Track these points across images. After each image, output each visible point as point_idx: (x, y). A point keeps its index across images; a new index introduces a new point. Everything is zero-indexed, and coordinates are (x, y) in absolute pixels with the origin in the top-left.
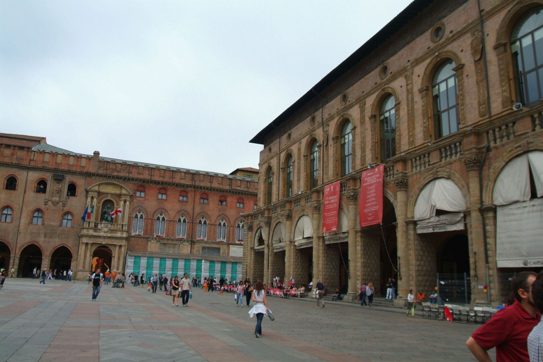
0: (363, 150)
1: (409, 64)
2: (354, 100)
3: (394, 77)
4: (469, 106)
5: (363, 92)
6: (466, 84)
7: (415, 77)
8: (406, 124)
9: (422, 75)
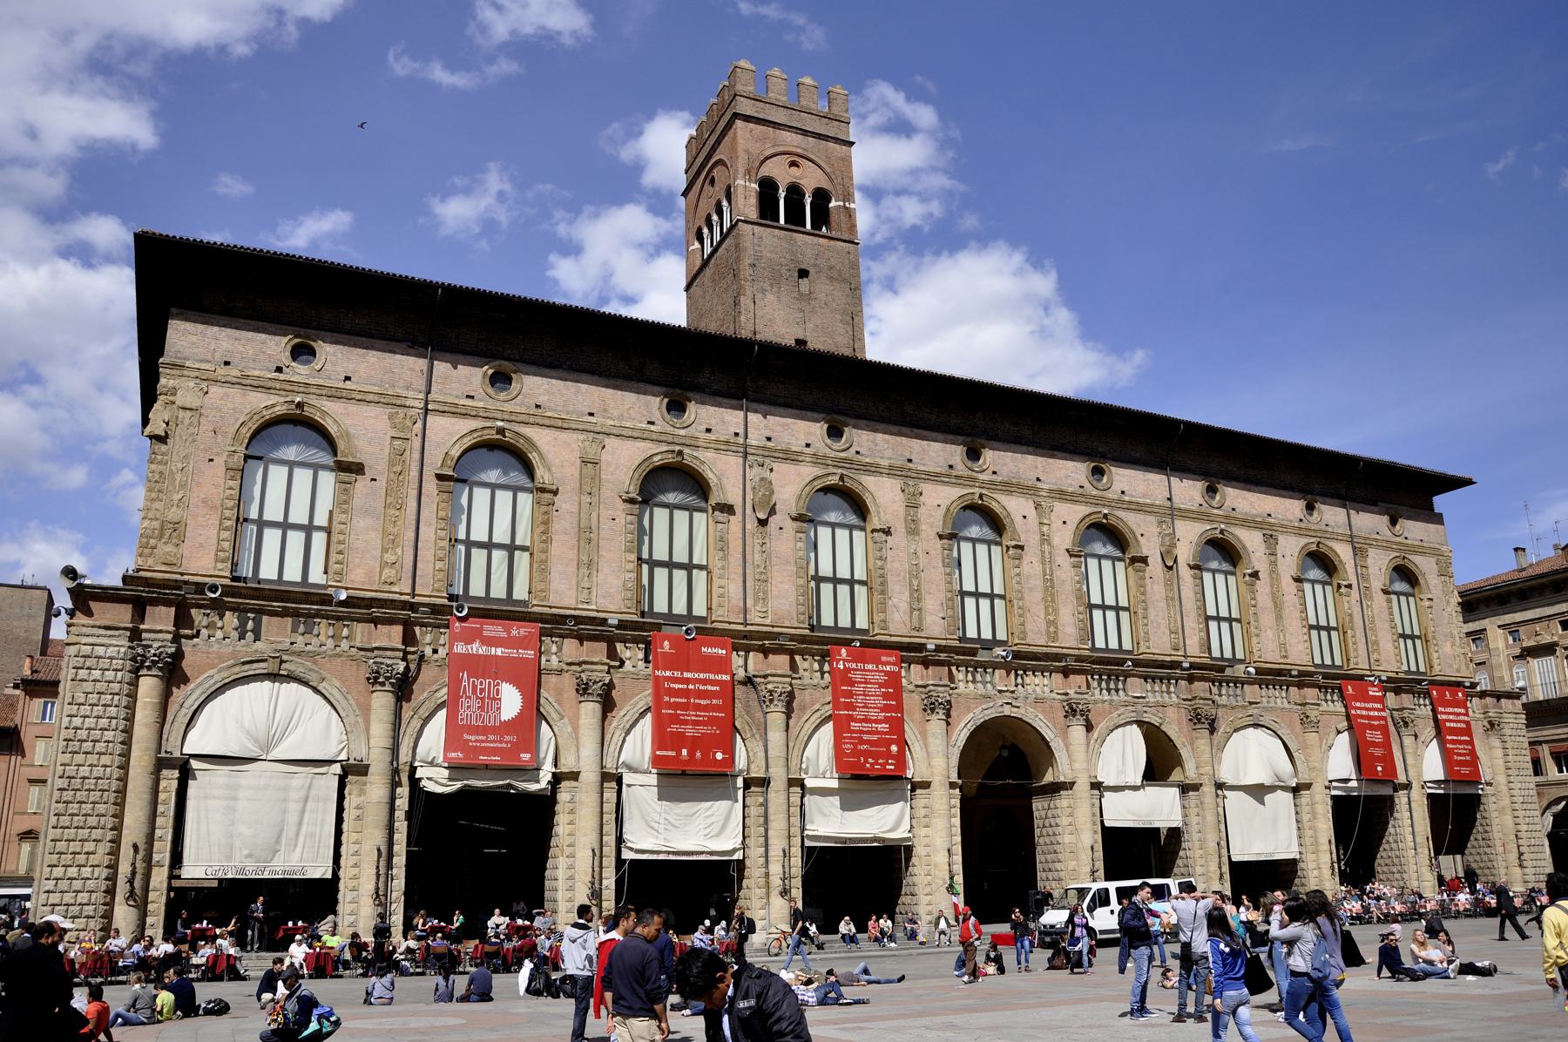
0: (916, 595)
1: (1039, 485)
2: (885, 463)
3: (1009, 487)
4: (1155, 625)
5: (910, 461)
6: (1148, 588)
7: (1057, 524)
8: (1039, 595)
9: (1072, 526)
